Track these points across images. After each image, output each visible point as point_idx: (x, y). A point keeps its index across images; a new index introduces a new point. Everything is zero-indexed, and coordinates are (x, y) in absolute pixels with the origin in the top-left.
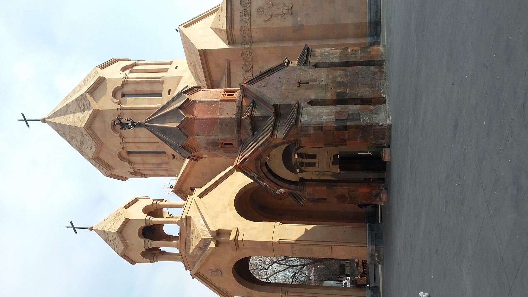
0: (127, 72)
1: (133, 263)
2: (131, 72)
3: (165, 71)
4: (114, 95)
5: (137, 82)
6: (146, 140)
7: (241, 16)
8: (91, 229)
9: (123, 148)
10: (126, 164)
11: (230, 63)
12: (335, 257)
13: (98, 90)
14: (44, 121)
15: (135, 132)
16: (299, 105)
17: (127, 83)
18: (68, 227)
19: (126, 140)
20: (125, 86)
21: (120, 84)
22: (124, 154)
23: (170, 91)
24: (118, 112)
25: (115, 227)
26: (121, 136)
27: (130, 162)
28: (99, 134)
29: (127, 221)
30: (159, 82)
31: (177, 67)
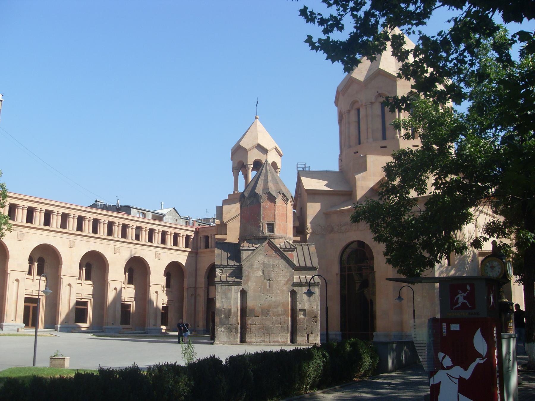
1: (232, 159)
16: (239, 283)
23: (385, 147)
26: (349, 111)
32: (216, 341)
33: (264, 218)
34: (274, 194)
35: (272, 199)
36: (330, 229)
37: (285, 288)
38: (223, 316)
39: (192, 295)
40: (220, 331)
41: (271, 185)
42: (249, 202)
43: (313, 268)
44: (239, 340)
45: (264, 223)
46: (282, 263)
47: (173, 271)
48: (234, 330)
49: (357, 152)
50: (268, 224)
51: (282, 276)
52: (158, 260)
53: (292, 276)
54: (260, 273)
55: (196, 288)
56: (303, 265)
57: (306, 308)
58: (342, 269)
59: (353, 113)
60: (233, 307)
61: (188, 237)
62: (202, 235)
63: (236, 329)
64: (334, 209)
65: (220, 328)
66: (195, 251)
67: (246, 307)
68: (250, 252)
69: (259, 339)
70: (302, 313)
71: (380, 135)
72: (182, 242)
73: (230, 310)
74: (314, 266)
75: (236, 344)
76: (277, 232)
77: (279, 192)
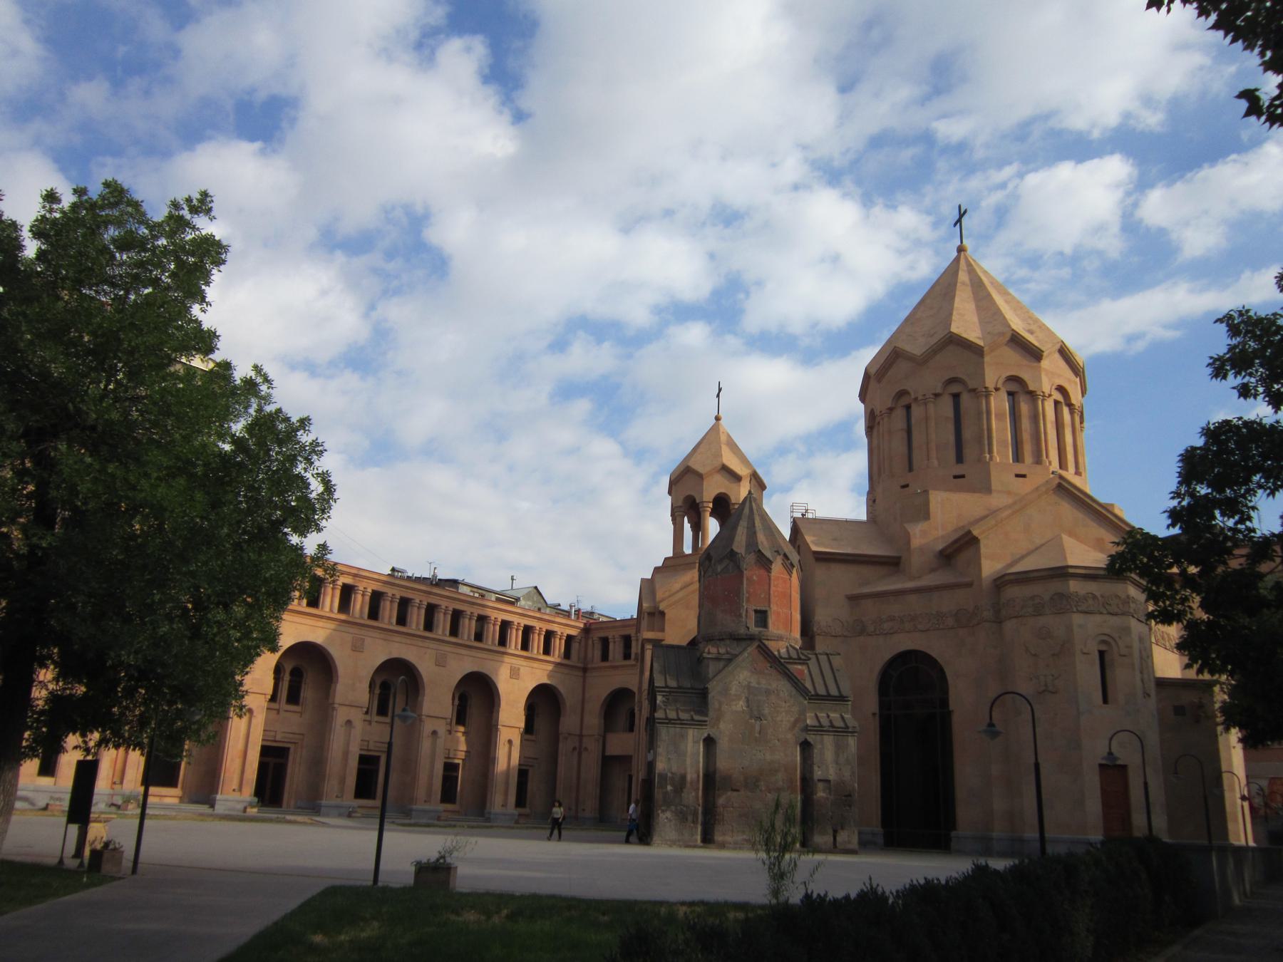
0: (1014, 387)
1: (670, 493)
2: (1010, 394)
3: (1018, 457)
5: (980, 414)
7: (1032, 598)
8: (718, 419)
11: (969, 585)
14: (961, 249)
22: (878, 419)
23: (963, 476)
25: (696, 465)
26: (891, 409)
29: (700, 476)
30: (982, 452)
31: (1024, 476)
32: (656, 839)
33: (748, 600)
34: (768, 554)
35: (765, 563)
36: (860, 630)
37: (789, 736)
38: (669, 788)
39: (574, 749)
40: (665, 819)
41: (761, 538)
42: (719, 568)
43: (841, 698)
44: (699, 838)
45: (749, 608)
46: (783, 686)
47: (543, 702)
48: (690, 818)
49: (907, 486)
50: (756, 611)
51: (785, 712)
52: (517, 680)
53: (802, 713)
54: (740, 705)
55: (581, 736)
56: (822, 691)
57: (831, 778)
58: (883, 705)
59: (900, 413)
60: (689, 770)
61: (569, 638)
62: (596, 635)
63: (695, 814)
64: (866, 590)
65: (663, 811)
66: (580, 665)
67: (715, 772)
68: (721, 664)
69: (740, 838)
70: (820, 785)
71: (951, 454)
72: (558, 646)
73: (683, 777)
74: (844, 694)
75: (695, 847)
76: (774, 627)
77: (777, 551)
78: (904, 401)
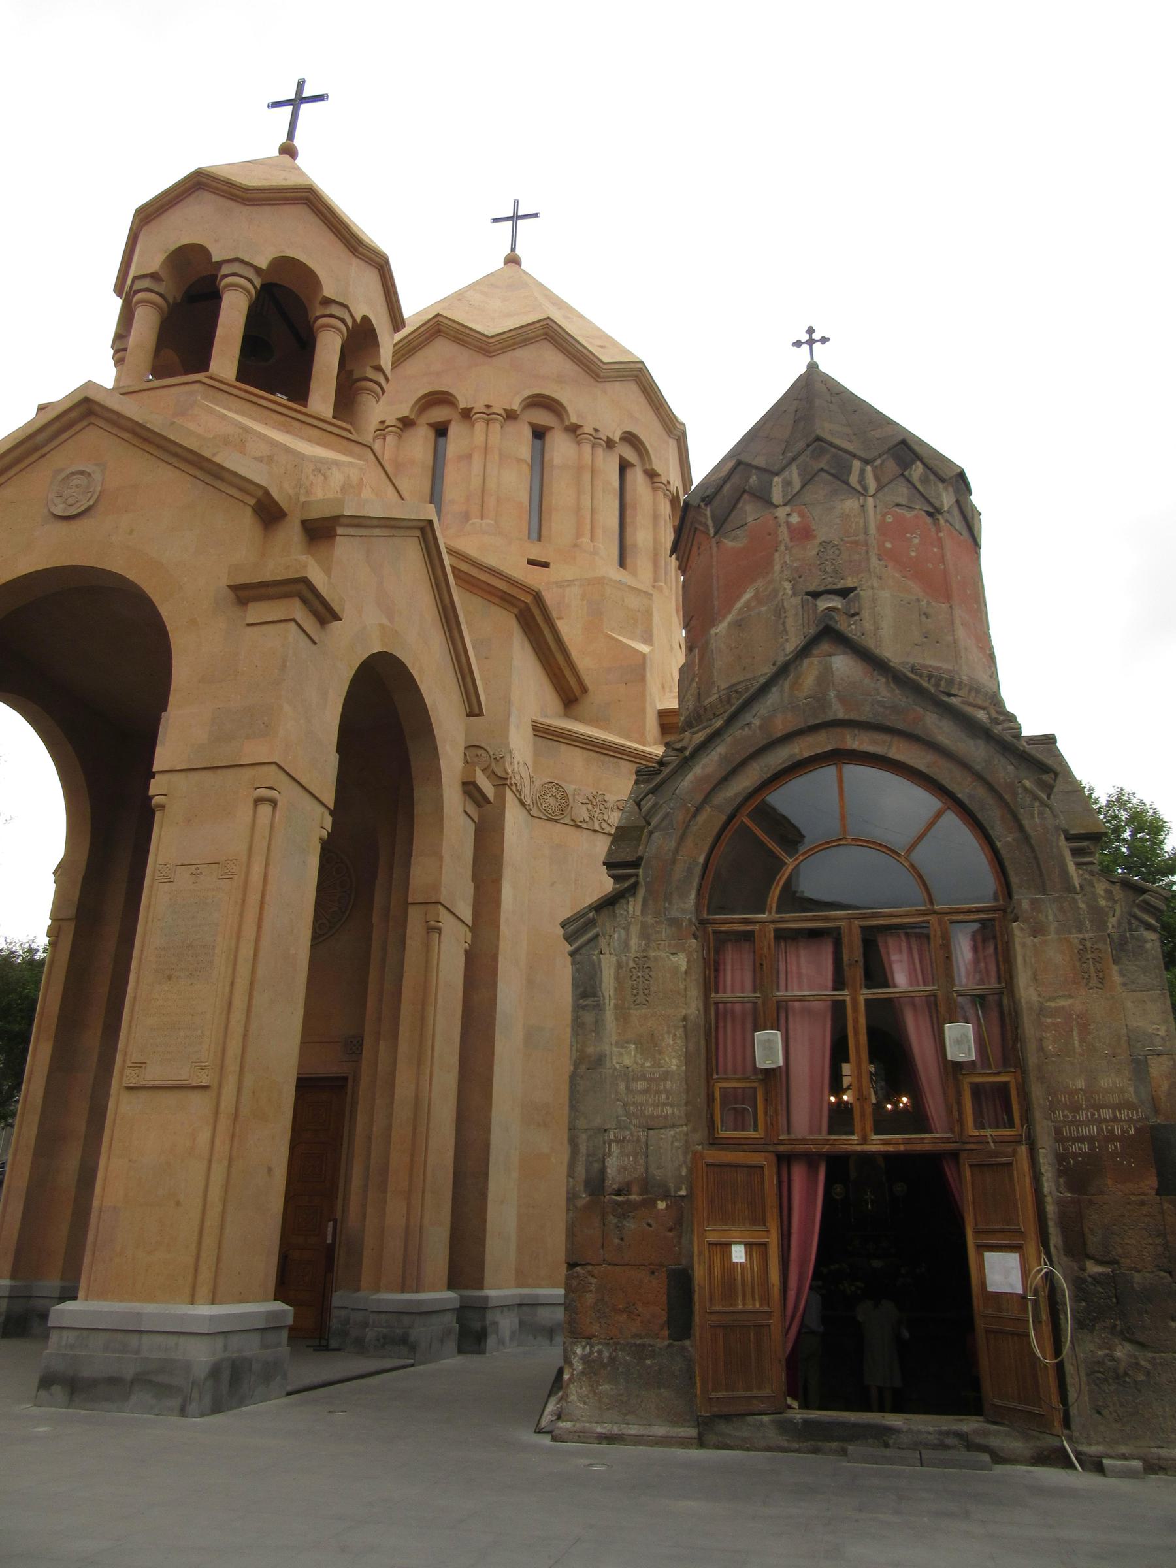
4: (631, 439)
6: (491, 485)
9: (467, 414)
10: (405, 410)
12: (122, 1107)
13: (642, 399)
14: (513, 260)
15: (519, 460)
17: (654, 489)
18: (301, 85)
19: (498, 426)
20: (648, 479)
21: (657, 466)
22: (439, 414)
24: (588, 429)
26: (511, 416)
27: (406, 423)
28: (522, 354)
49: (546, 565)
78: (543, 418)
